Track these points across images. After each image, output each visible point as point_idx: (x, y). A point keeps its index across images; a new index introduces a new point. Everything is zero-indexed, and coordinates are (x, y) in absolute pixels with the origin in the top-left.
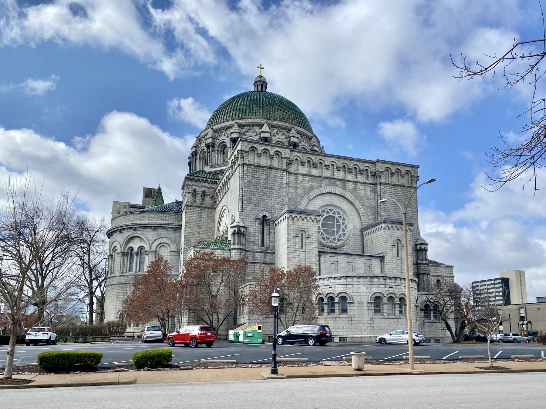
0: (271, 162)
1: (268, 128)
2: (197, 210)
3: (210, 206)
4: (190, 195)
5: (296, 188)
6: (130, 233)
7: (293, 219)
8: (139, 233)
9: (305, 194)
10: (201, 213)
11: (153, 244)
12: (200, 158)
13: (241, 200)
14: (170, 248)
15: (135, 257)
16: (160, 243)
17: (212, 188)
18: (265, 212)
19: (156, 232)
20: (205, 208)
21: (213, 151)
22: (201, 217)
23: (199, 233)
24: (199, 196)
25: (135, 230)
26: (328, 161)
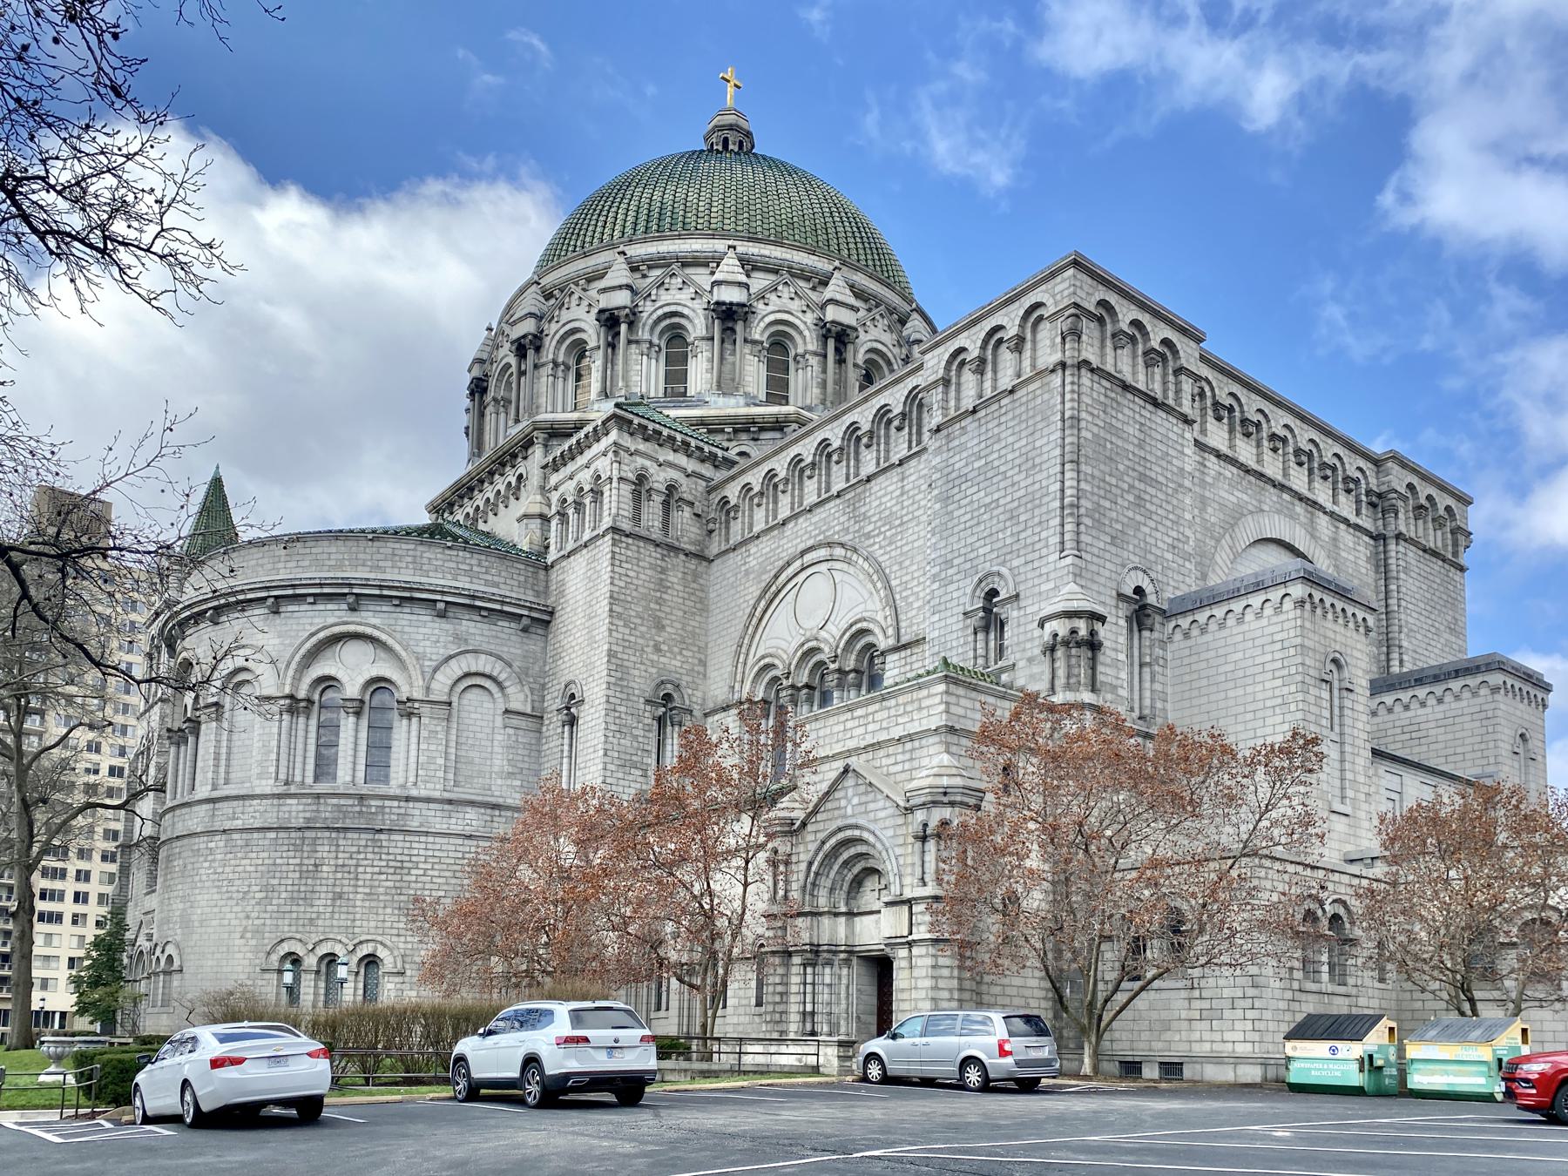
2: (651, 555)
4: (627, 489)
5: (1203, 502)
6: (332, 617)
7: (1314, 608)
8: (374, 621)
9: (1226, 530)
10: (663, 571)
11: (439, 676)
12: (556, 364)
13: (1071, 509)
14: (504, 695)
16: (467, 675)
17: (701, 477)
18: (1140, 574)
19: (445, 625)
20: (672, 548)
22: (662, 586)
23: (657, 649)
24: (658, 499)
25: (353, 609)
26: (1279, 421)
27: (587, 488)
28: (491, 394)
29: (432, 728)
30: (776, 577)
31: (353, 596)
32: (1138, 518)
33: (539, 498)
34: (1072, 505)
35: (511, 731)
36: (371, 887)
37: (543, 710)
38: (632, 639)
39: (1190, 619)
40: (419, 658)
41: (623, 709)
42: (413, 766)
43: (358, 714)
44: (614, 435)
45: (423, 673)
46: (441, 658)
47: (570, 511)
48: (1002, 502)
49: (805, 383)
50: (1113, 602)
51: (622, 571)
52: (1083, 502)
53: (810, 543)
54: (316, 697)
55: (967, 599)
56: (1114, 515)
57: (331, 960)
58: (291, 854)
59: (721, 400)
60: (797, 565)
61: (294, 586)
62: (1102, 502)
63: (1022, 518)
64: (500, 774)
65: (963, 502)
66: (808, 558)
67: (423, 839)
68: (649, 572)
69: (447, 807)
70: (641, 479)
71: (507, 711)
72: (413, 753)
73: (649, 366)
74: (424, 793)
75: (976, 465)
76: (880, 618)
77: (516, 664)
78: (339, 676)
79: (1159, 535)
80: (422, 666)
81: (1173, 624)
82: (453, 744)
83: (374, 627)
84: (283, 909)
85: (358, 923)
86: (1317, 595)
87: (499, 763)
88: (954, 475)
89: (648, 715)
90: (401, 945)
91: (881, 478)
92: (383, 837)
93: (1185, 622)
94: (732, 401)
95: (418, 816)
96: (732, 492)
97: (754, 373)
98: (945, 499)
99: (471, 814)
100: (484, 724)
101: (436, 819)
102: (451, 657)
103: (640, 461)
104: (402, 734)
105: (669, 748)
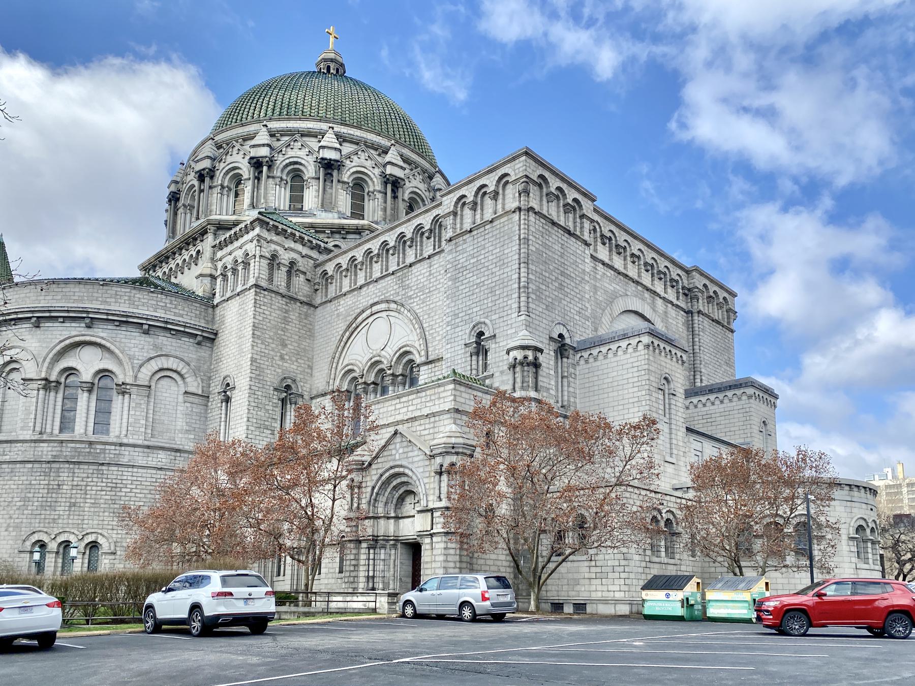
0: (566, 219)
1: (399, 158)
2: (279, 302)
3: (305, 299)
4: (265, 263)
6: (75, 331)
7: (654, 349)
8: (102, 335)
10: (287, 312)
11: (143, 369)
12: (223, 187)
14: (184, 382)
15: (83, 397)
17: (311, 258)
18: (562, 327)
20: (293, 299)
21: (268, 177)
22: (286, 320)
23: (282, 358)
24: (284, 269)
25: (88, 327)
26: (636, 246)
27: (240, 260)
28: (182, 201)
29: (138, 401)
30: (356, 319)
31: (90, 320)
32: (560, 295)
33: (210, 265)
34: (524, 287)
35: (189, 405)
36: (95, 499)
37: (209, 392)
38: (267, 351)
39: (589, 353)
40: (131, 358)
41: (260, 393)
42: (125, 425)
43: (90, 391)
44: (257, 230)
45: (133, 367)
46: (145, 359)
47: (229, 274)
48: (486, 283)
49: (374, 208)
50: (547, 342)
51: (261, 311)
52: (530, 285)
53: (376, 300)
54: (63, 380)
55: (467, 337)
56: (547, 293)
57: (66, 544)
58: (42, 478)
59: (324, 214)
60: (368, 312)
61: (50, 311)
62: (541, 286)
63: (497, 292)
64: (181, 431)
65: (465, 282)
66: (375, 309)
67: (130, 470)
68: (278, 312)
69: (146, 450)
70: (274, 256)
71: (186, 393)
72: (125, 416)
73: (280, 191)
74: (131, 441)
75: (472, 261)
76: (417, 345)
77: (192, 364)
78: (78, 368)
79: (571, 306)
80: (132, 363)
81: (579, 355)
82: (151, 412)
83: (102, 338)
84: (35, 512)
85: (86, 522)
86: (656, 342)
87: (181, 424)
88: (459, 266)
89: (275, 398)
90: (114, 536)
91: (418, 265)
92: (104, 468)
93: (585, 354)
94: (330, 215)
95: (127, 455)
96: (330, 268)
97: (344, 200)
98: (454, 279)
99: (162, 455)
100: (172, 400)
101: (139, 458)
102: (151, 358)
103: (273, 247)
104: (118, 404)
105: (288, 417)
